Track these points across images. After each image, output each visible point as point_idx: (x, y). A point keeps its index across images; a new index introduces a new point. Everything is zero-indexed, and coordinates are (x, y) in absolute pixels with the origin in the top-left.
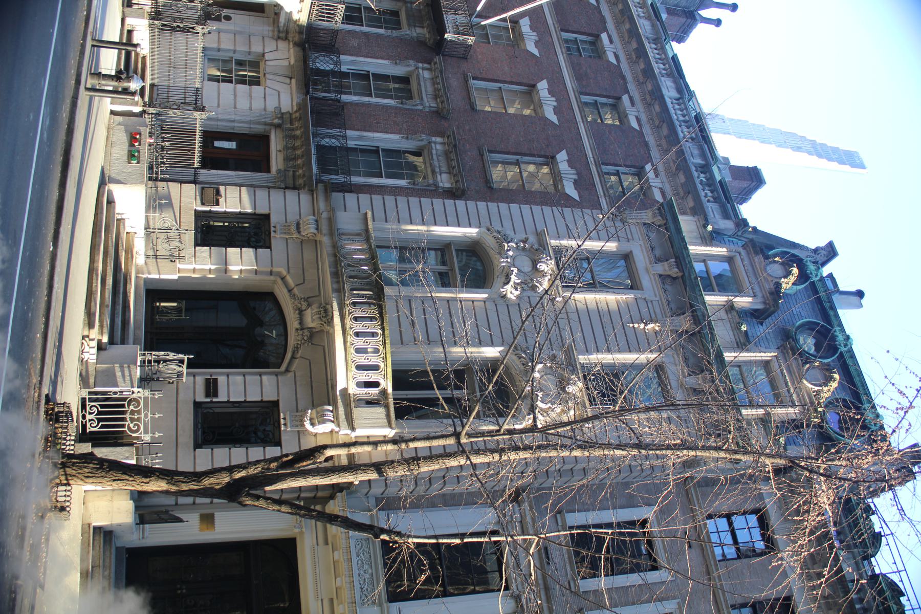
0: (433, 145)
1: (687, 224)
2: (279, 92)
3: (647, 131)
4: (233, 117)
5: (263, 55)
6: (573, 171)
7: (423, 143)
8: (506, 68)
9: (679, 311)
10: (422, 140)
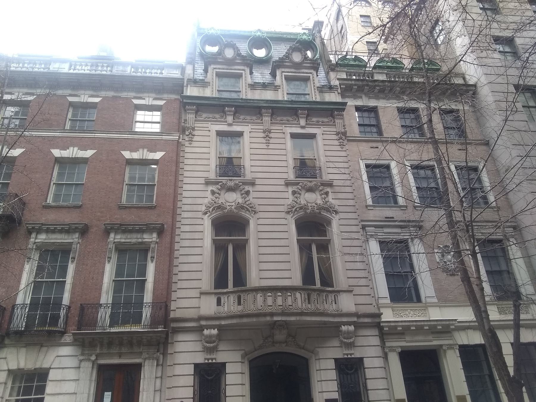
0: (116, 240)
1: (191, 91)
2: (58, 356)
3: (103, 93)
4: (86, 395)
5: (10, 371)
6: (141, 150)
7: (114, 247)
8: (37, 176)
9: (261, 115)
10: (113, 247)
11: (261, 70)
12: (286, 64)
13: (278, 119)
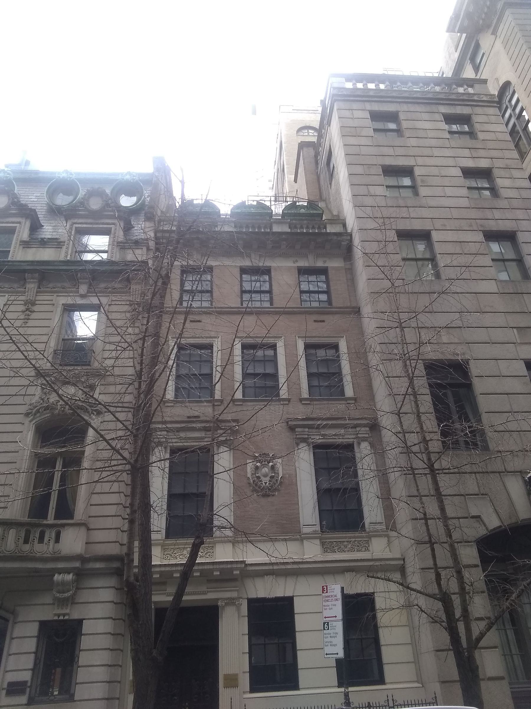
11: (56, 222)
12: (80, 213)
13: (51, 285)
